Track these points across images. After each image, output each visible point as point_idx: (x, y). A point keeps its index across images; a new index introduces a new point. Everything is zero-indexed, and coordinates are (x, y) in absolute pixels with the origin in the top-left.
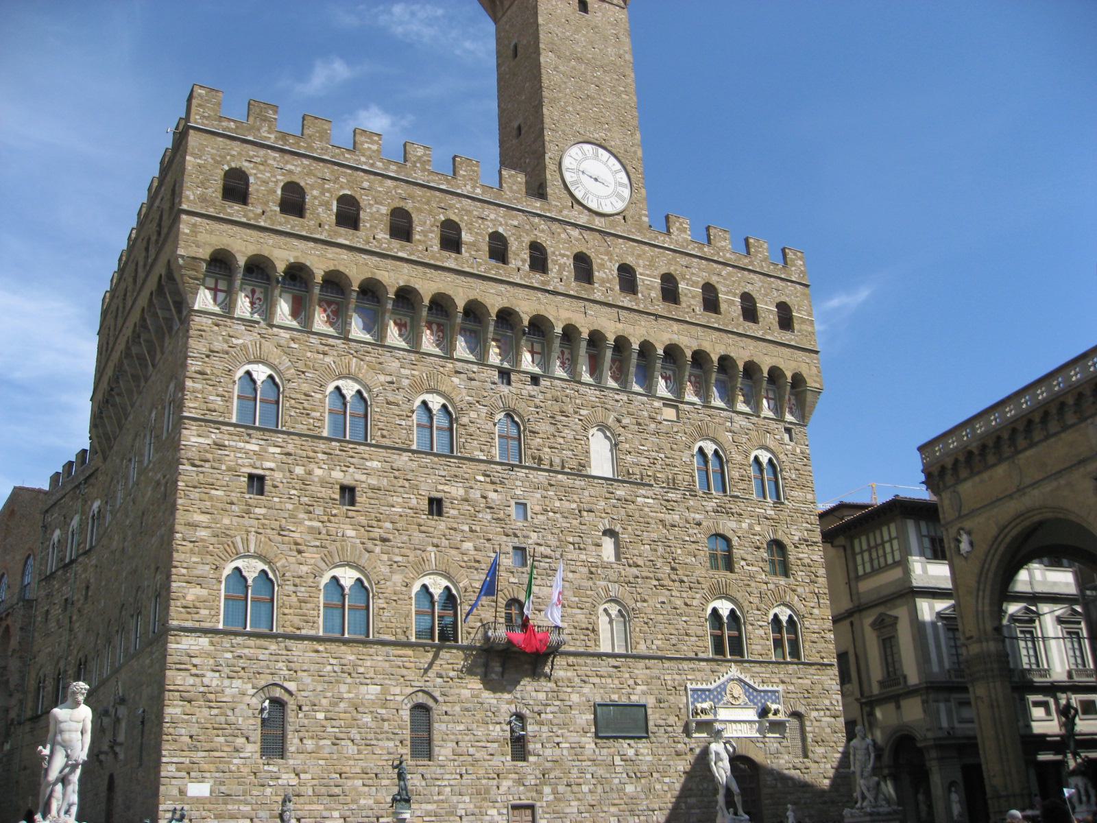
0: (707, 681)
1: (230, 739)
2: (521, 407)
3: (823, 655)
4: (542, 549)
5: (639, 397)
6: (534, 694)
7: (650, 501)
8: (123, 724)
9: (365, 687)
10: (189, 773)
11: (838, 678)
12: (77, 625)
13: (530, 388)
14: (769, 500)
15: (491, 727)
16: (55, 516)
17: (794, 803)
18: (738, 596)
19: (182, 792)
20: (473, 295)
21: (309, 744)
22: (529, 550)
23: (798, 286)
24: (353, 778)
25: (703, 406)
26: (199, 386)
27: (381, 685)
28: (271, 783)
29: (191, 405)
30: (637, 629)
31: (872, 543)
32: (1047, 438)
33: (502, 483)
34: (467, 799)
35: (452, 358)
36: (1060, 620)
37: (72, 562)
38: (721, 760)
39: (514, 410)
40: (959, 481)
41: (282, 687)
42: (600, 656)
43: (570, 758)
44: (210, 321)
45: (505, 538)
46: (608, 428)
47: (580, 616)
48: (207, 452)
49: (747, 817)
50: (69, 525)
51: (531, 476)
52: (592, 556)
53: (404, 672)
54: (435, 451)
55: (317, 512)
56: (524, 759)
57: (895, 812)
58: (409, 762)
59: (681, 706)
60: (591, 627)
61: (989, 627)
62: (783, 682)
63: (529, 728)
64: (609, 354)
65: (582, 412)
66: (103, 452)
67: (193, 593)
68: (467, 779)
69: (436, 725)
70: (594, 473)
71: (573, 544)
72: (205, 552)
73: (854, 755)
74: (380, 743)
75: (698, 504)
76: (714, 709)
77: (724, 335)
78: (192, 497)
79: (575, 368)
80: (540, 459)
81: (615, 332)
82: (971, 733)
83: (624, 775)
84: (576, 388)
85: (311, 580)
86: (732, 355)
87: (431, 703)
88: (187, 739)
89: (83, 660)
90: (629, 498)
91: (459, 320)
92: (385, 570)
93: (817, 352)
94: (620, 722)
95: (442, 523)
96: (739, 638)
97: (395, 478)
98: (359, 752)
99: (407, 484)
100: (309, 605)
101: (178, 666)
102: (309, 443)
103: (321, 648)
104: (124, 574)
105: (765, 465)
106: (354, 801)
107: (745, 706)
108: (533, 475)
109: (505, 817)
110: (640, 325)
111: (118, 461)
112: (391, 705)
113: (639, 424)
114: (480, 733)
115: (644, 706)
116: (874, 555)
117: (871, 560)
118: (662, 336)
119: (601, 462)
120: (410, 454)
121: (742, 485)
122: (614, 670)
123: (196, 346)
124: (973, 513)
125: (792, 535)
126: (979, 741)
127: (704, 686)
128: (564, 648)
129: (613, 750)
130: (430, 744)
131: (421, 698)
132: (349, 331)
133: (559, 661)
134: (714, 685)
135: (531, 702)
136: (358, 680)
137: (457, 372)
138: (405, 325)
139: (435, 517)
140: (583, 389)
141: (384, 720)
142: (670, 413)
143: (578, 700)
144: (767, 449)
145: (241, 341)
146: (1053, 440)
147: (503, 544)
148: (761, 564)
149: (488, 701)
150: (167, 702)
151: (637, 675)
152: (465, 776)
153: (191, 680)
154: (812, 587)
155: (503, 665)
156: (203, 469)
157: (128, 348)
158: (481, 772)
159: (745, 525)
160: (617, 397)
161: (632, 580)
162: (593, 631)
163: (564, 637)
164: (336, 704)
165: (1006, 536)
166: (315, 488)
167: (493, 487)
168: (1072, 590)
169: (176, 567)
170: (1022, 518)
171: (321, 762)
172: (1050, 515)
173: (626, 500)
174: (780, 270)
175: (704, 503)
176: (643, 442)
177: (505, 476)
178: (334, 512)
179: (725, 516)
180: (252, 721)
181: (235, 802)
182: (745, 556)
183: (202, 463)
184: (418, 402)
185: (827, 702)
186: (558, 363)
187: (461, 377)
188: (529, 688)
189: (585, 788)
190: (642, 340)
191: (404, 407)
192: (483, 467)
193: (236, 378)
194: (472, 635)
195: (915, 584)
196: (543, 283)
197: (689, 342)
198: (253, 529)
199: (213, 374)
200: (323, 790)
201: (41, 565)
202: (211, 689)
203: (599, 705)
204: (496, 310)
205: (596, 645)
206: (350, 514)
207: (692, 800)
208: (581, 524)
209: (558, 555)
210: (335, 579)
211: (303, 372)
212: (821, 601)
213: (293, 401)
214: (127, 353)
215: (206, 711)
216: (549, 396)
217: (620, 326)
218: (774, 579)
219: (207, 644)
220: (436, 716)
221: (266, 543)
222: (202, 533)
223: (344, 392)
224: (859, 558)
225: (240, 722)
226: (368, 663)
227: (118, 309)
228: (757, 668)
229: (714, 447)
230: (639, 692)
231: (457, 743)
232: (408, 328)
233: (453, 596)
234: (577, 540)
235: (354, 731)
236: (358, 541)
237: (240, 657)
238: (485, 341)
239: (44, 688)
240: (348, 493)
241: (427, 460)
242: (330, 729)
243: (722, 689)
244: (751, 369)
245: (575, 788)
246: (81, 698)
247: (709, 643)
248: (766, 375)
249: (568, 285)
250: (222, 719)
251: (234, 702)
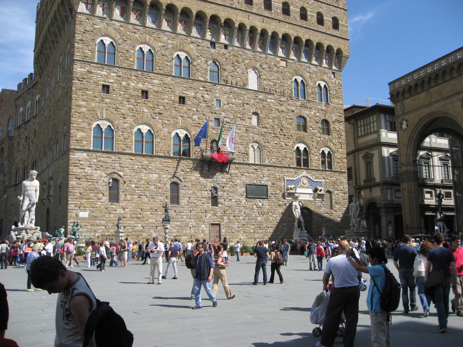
0: (293, 177)
1: (96, 194)
2: (220, 58)
3: (342, 168)
4: (227, 119)
5: (271, 56)
6: (221, 179)
7: (273, 101)
8: (52, 188)
10: (79, 208)
11: (347, 178)
12: (31, 147)
13: (224, 50)
14: (323, 102)
15: (203, 192)
16: (20, 102)
17: (326, 227)
18: (308, 142)
19: (77, 215)
20: (200, 8)
21: (129, 197)
22: (221, 120)
23: (342, 10)
24: (147, 211)
25: (298, 61)
26: (80, 46)
27: (158, 174)
28: (113, 212)
29: (77, 54)
30: (265, 154)
31: (366, 123)
32: (444, 82)
33: (210, 91)
34: (193, 220)
35: (190, 36)
36: (440, 159)
37: (28, 121)
38: (297, 209)
39: (216, 60)
40: (404, 98)
41: (117, 174)
42: (249, 164)
43: (235, 206)
44: (85, 18)
45: (211, 114)
46: (257, 69)
47: (242, 148)
48: (84, 74)
49: (306, 232)
50: (26, 105)
51: (223, 88)
52: (248, 123)
53: (168, 169)
54: (182, 76)
55: (132, 101)
56: (217, 206)
57: (366, 232)
58: (169, 205)
59: (282, 186)
60: (246, 153)
61: (411, 160)
62: (324, 178)
63: (219, 193)
64: (258, 37)
65: (246, 62)
66: (40, 74)
67: (80, 135)
68: (193, 213)
69: (181, 191)
70: (250, 88)
71: (240, 118)
72: (84, 117)
73: (351, 209)
74: (158, 197)
75: (293, 103)
76: (295, 188)
77: (308, 30)
78: (79, 94)
79: (243, 43)
80: (227, 81)
81: (261, 27)
82: (399, 203)
83: (257, 213)
84: (243, 51)
85: (129, 130)
86: (311, 39)
87: (179, 182)
88: (79, 194)
89: (34, 162)
90: (264, 99)
91: (194, 20)
92: (160, 126)
93: (348, 40)
94: (256, 192)
95: (185, 107)
96: (307, 159)
97: (165, 87)
98: (149, 201)
99: (170, 90)
100: (128, 140)
101: (74, 165)
102: (128, 72)
103: (133, 158)
104: (51, 126)
105: (322, 88)
106: (147, 220)
107: (308, 188)
108: (224, 88)
109: (208, 228)
110: (272, 24)
111: (46, 78)
112: (162, 182)
113: (270, 68)
114: (199, 194)
115: (267, 186)
116: (366, 128)
117: (365, 130)
118: (282, 30)
119: (253, 83)
120: (171, 77)
121: (312, 96)
122: (255, 171)
123: (79, 28)
124: (409, 112)
125: (332, 118)
126: (403, 206)
127: (292, 179)
128: (234, 161)
129: (253, 203)
130: (178, 198)
131: (175, 180)
132: (145, 23)
133: (232, 166)
134: (296, 178)
135: (220, 183)
136: (149, 172)
137: (192, 42)
138: (170, 21)
139: (182, 105)
140: (246, 52)
141: (159, 188)
142: (283, 64)
143: (239, 182)
144: (324, 81)
145: (98, 27)
146: (446, 83)
147: (210, 117)
148: (318, 129)
149: (202, 181)
150: (70, 179)
151: (264, 173)
152: (192, 212)
153: (80, 170)
154: (339, 140)
155: (209, 167)
156: (83, 82)
157: (49, 29)
158: (199, 210)
159: (312, 113)
160: (261, 55)
161: (264, 134)
162: (247, 154)
163: (235, 156)
164: (140, 181)
165: (422, 123)
166: (131, 91)
167: (206, 92)
168: (447, 147)
169: (72, 124)
170: (429, 116)
171: (133, 204)
172: (441, 115)
173: (263, 100)
174: (335, 2)
175: (296, 103)
176: (271, 75)
177: (212, 88)
178: (139, 101)
179: (304, 108)
180: (105, 187)
181: (99, 220)
182: (312, 126)
183: (83, 80)
184: (175, 55)
185: (342, 187)
186: (236, 40)
187: (193, 44)
188: (219, 177)
189: (241, 218)
190: (273, 31)
191: (169, 57)
192: (202, 84)
193: (97, 43)
194: (196, 154)
195: (382, 141)
196: (231, 4)
197: (293, 33)
198: (105, 108)
199: (86, 41)
200: (134, 216)
201: (15, 122)
202: (88, 174)
203: (248, 185)
204: (210, 15)
205: (248, 160)
206: (146, 102)
207: (284, 224)
208: (243, 109)
209: (233, 122)
210: (139, 130)
211: (126, 41)
212: (342, 146)
213: (121, 54)
214: (49, 31)
215: (86, 183)
216: (231, 54)
217: (264, 24)
218: (324, 136)
219: (86, 156)
220: (181, 187)
221: (110, 114)
222: (83, 110)
223: (144, 50)
224: (359, 129)
225: (100, 188)
226: (153, 165)
227: (44, 11)
228: (314, 172)
229: (302, 79)
230: (265, 180)
231: (189, 198)
232: (171, 23)
233: (189, 138)
234: (242, 116)
235: (147, 192)
236: (149, 114)
237: (100, 161)
238: (205, 29)
239: (19, 173)
240: (145, 93)
241: (179, 80)
242: (137, 191)
243: (299, 180)
244: (319, 46)
245: (237, 218)
246: (35, 177)
247: (295, 161)
248: (325, 48)
249: (241, 6)
250: (93, 186)
251: (97, 180)
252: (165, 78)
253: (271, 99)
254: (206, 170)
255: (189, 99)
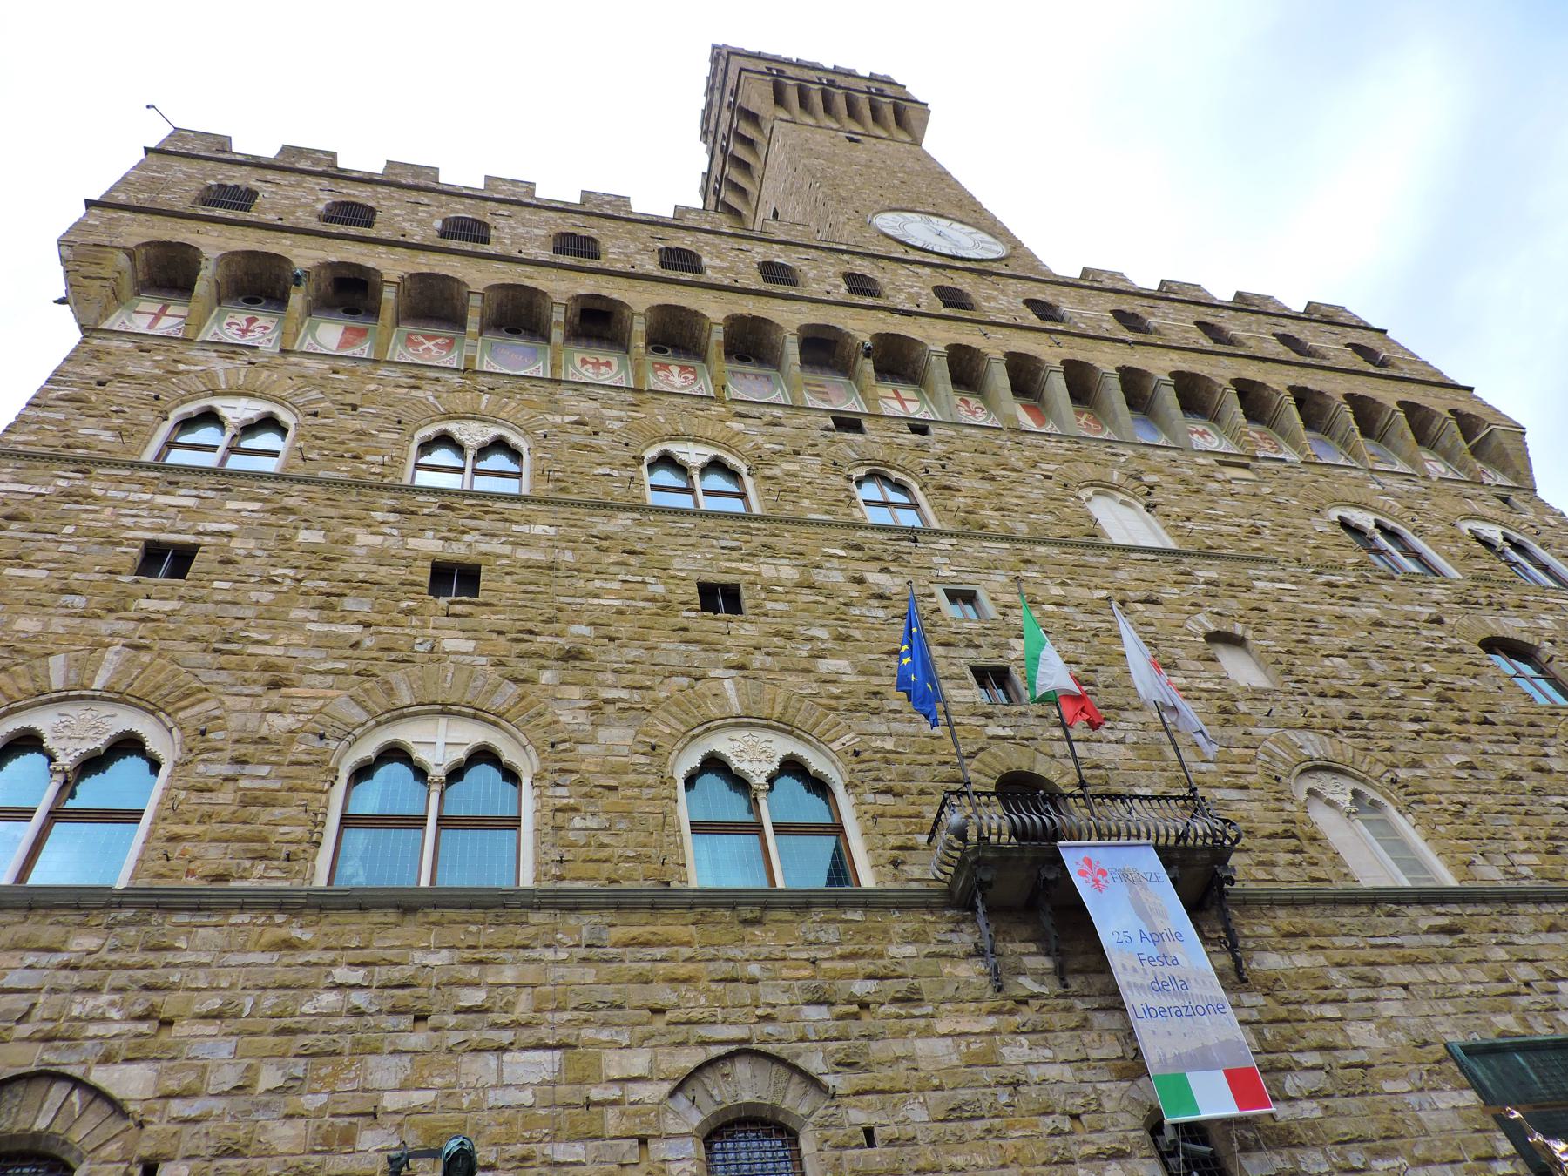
5: (1159, 452)
9: (491, 1059)
39: (885, 464)
42: (1375, 899)
51: (970, 550)
87: (794, 1102)
92: (570, 717)
95: (747, 626)
112: (612, 1121)
120: (637, 516)
122: (1447, 940)
131: (747, 1086)
140: (1028, 439)
143: (1380, 1044)
167: (876, 565)
252: (595, 519)
253: (1272, 580)
254: (1038, 976)
255: (769, 592)
